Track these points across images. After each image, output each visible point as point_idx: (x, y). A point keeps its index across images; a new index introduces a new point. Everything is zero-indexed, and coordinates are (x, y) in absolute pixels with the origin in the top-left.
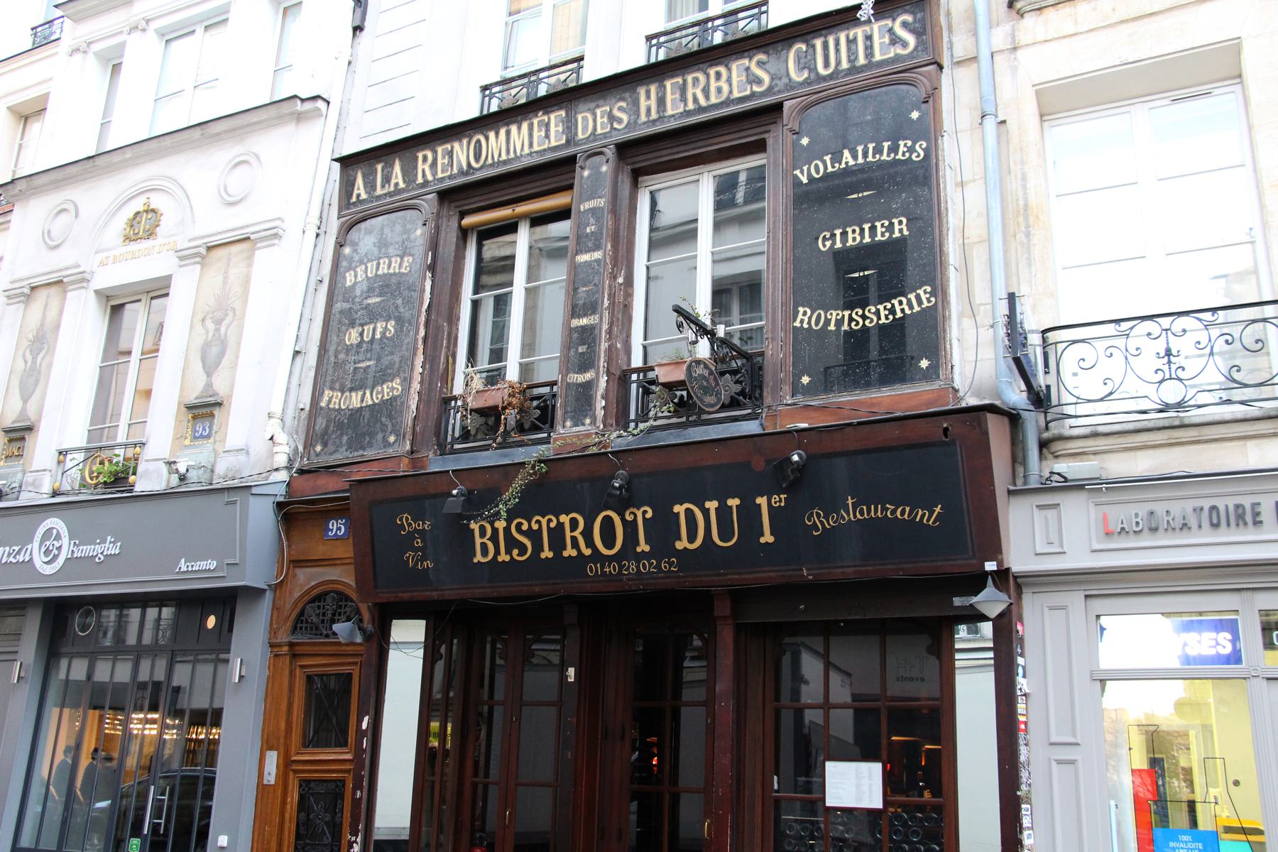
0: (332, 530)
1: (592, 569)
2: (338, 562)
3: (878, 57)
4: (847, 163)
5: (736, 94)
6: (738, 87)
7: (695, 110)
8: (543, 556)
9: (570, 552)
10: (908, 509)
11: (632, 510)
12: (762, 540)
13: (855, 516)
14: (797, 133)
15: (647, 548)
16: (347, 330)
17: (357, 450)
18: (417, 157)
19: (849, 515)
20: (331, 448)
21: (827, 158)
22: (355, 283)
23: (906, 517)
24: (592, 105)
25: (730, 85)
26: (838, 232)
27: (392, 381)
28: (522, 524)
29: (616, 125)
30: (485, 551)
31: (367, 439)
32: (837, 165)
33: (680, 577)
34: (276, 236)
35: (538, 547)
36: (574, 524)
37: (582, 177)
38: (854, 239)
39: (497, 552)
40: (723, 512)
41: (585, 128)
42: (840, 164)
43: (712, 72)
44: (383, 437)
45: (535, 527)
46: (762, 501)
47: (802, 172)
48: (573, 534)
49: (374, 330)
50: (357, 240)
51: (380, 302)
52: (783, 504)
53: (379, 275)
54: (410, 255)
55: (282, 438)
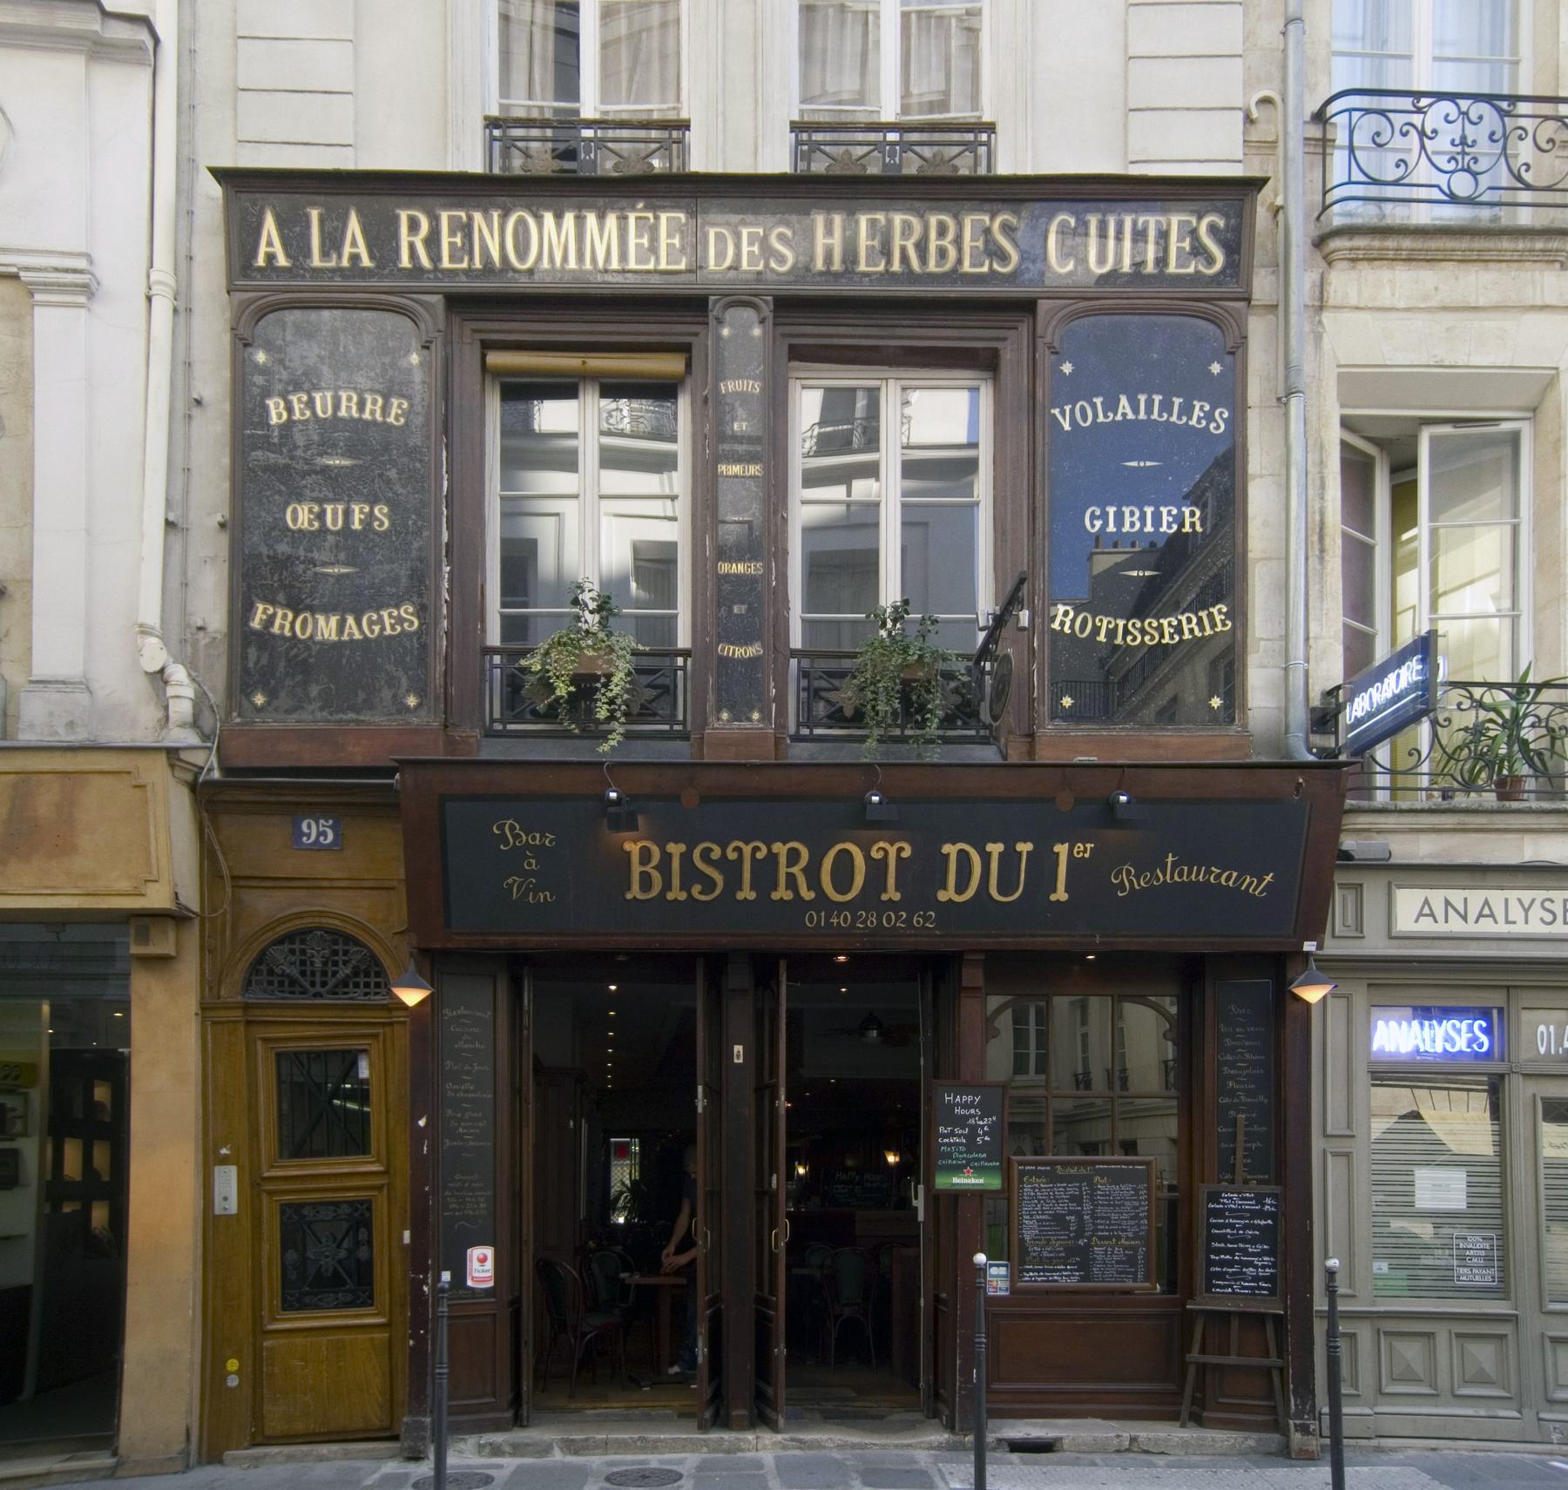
0: (309, 836)
1: (812, 919)
2: (325, 884)
3: (1172, 268)
4: (1124, 415)
5: (967, 267)
6: (971, 255)
7: (903, 274)
8: (740, 896)
9: (782, 893)
10: (1235, 874)
11: (881, 844)
12: (1053, 897)
13: (1172, 878)
14: (1057, 353)
15: (897, 897)
16: (287, 504)
17: (344, 712)
18: (397, 217)
19: (1165, 875)
20: (284, 700)
21: (1098, 401)
22: (289, 421)
23: (1231, 883)
24: (735, 218)
25: (960, 250)
26: (1111, 510)
27: (397, 607)
28: (711, 850)
29: (773, 265)
30: (646, 882)
31: (362, 696)
32: (1111, 415)
33: (936, 935)
34: (88, 290)
35: (734, 882)
36: (793, 857)
37: (719, 337)
38: (1132, 524)
39: (667, 886)
40: (1009, 858)
41: (721, 255)
42: (1115, 414)
43: (933, 220)
44: (394, 696)
45: (732, 856)
46: (1062, 849)
47: (1063, 413)
48: (791, 870)
49: (348, 514)
50: (279, 342)
51: (352, 468)
52: (1087, 855)
53: (343, 419)
54: (403, 396)
55: (178, 673)
